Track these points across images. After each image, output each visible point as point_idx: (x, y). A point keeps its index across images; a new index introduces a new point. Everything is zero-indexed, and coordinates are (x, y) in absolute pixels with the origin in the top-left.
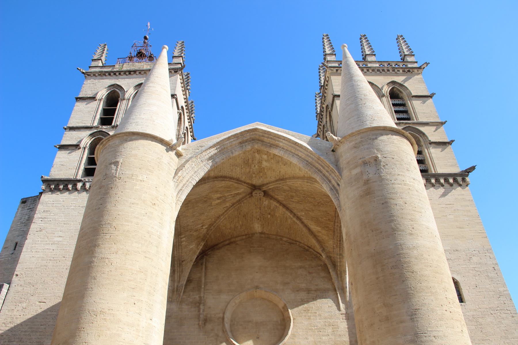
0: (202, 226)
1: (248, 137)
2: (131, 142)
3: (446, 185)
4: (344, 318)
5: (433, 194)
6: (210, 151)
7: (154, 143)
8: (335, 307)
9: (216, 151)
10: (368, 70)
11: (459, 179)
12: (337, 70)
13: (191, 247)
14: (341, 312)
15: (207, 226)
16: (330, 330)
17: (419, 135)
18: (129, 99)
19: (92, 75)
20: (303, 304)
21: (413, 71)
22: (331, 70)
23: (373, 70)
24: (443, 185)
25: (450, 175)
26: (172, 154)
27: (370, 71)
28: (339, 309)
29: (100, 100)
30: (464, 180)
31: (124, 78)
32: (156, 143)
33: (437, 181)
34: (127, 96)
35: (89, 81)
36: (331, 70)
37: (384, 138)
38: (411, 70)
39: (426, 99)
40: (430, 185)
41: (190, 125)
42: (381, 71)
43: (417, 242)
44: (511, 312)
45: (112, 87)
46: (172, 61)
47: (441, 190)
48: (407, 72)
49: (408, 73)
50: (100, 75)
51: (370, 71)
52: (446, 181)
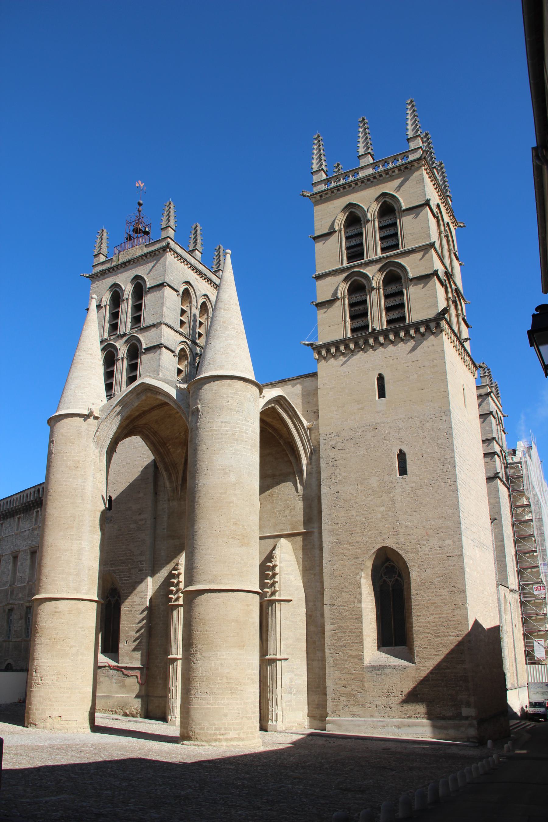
0: (180, 434)
1: (140, 390)
2: (59, 423)
3: (418, 336)
4: (302, 499)
5: (400, 351)
6: (116, 409)
7: (74, 418)
8: (294, 490)
9: (120, 408)
10: (356, 184)
11: (432, 325)
12: (321, 196)
13: (178, 452)
14: (298, 494)
15: (183, 433)
16: (287, 512)
17: (401, 270)
18: (128, 299)
19: (95, 277)
20: (269, 490)
21: (412, 166)
22: (315, 197)
23: (362, 182)
24: (413, 338)
25: (422, 323)
26: (91, 420)
27: (359, 184)
28: (297, 491)
29: (106, 306)
30: (438, 326)
31: (122, 272)
32: (75, 418)
33: (407, 333)
34: (125, 296)
35: (94, 284)
36: (315, 197)
37: (206, 387)
38: (409, 166)
39: (421, 209)
40: (399, 340)
41: (214, 286)
42: (372, 179)
43: (208, 480)
44: (451, 481)
45: (113, 287)
46: (160, 236)
47: (412, 343)
48: (404, 171)
49: (406, 170)
50: (101, 274)
51: (359, 184)
52: (417, 331)
